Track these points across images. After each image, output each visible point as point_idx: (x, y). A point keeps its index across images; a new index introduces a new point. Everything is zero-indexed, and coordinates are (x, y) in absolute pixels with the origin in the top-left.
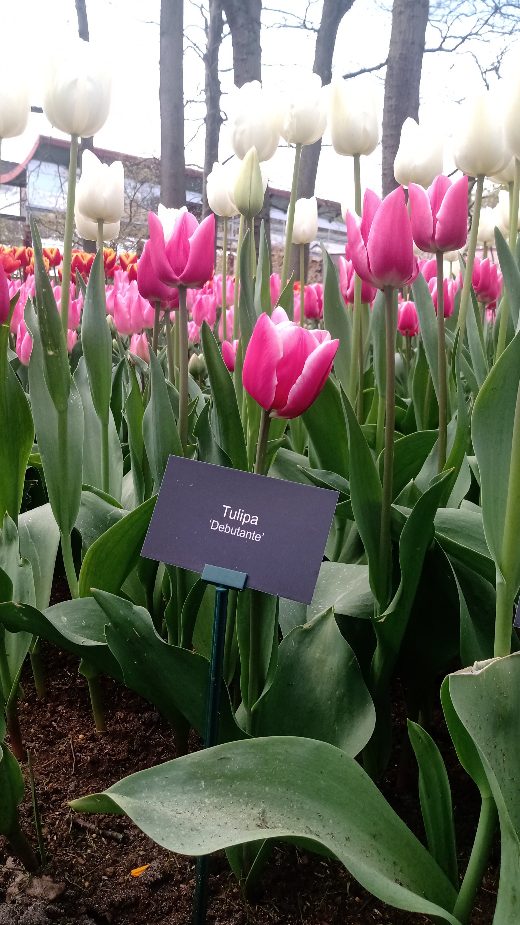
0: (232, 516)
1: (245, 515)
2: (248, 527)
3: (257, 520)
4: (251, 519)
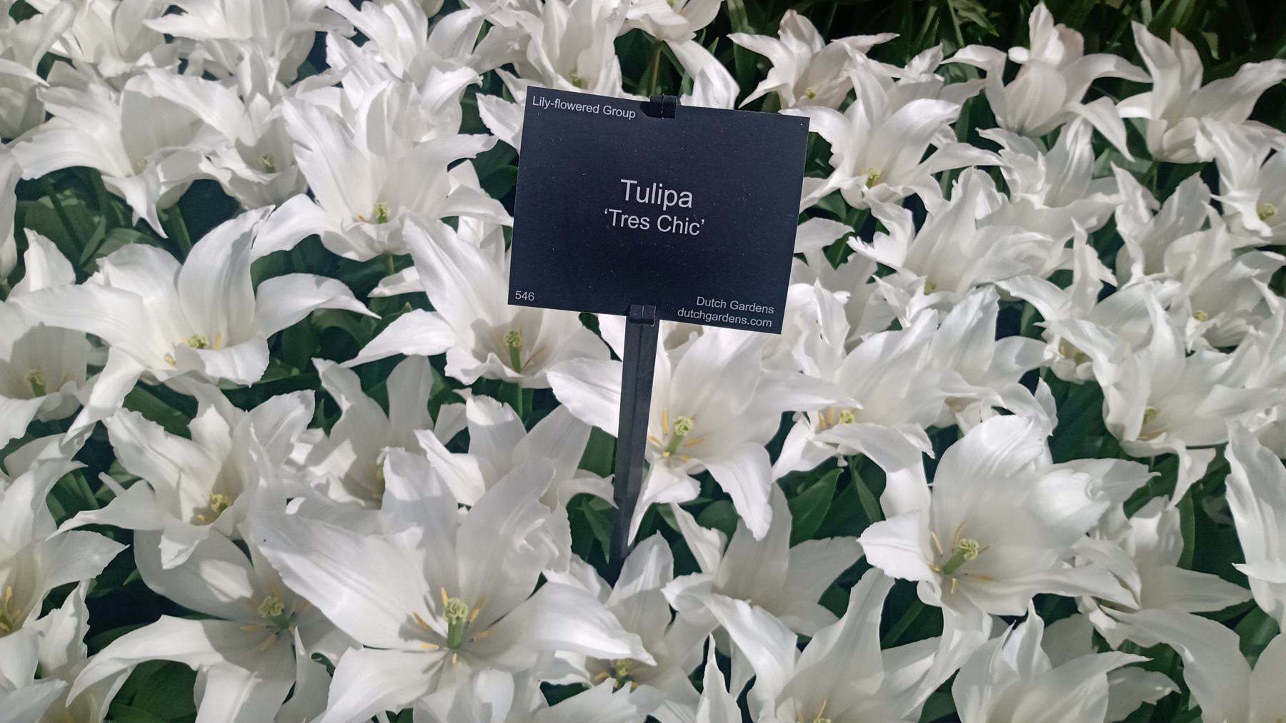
0: (642, 197)
1: (667, 192)
3: (690, 199)
4: (679, 198)
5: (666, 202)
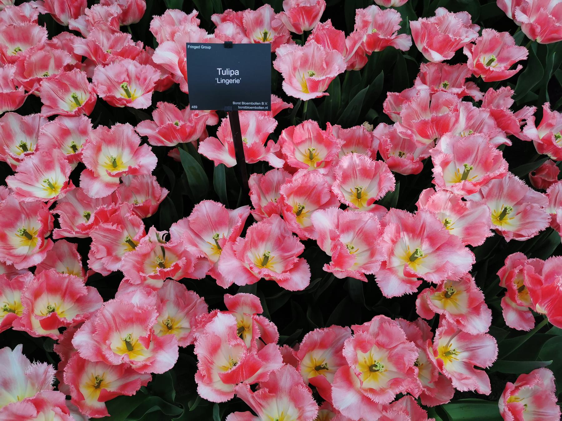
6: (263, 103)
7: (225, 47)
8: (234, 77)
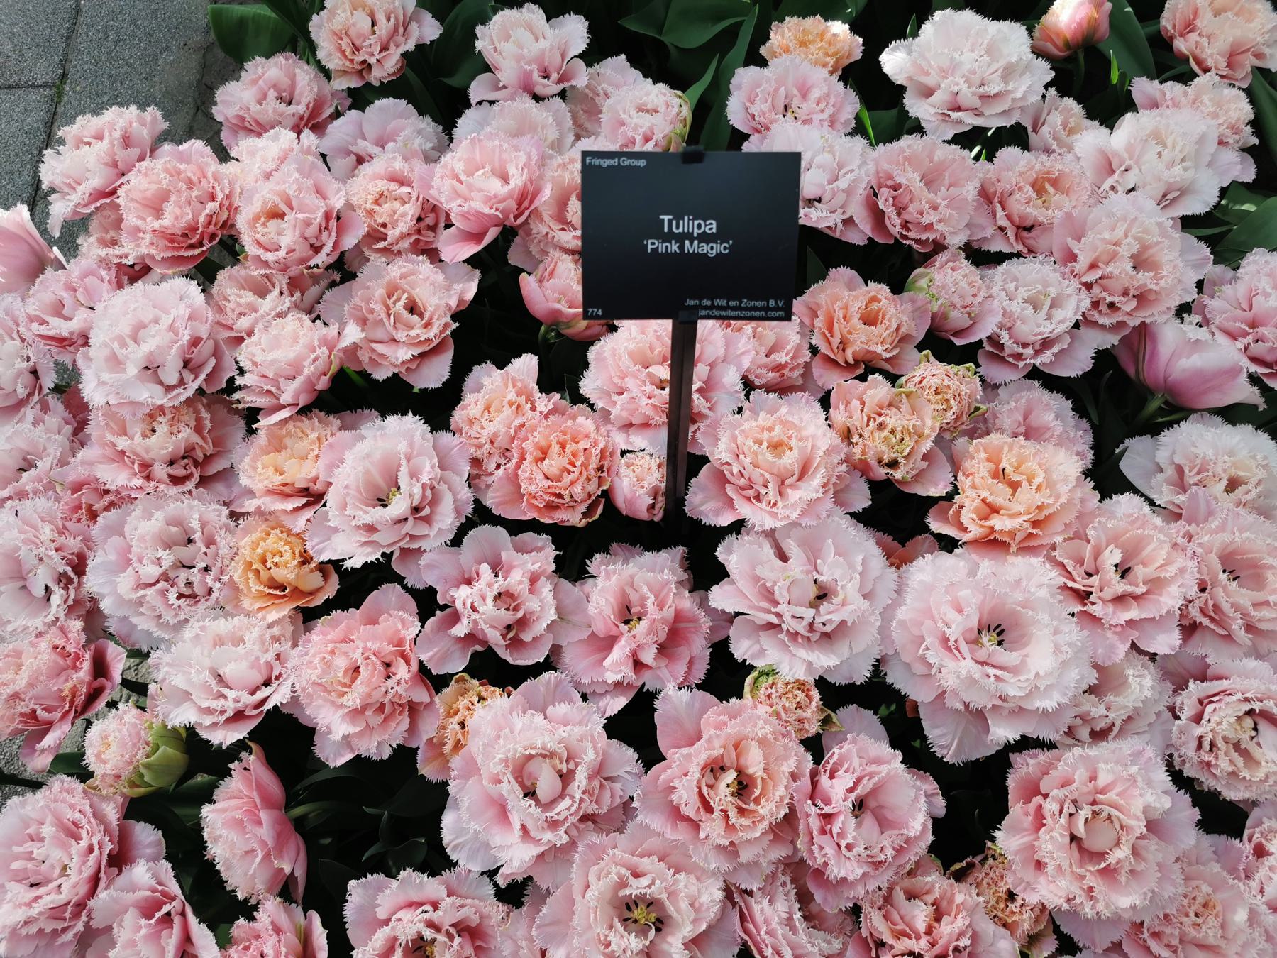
0: (678, 227)
2: (704, 238)
3: (714, 226)
5: (696, 231)
6: (772, 303)
7: (685, 162)
8: (704, 238)
